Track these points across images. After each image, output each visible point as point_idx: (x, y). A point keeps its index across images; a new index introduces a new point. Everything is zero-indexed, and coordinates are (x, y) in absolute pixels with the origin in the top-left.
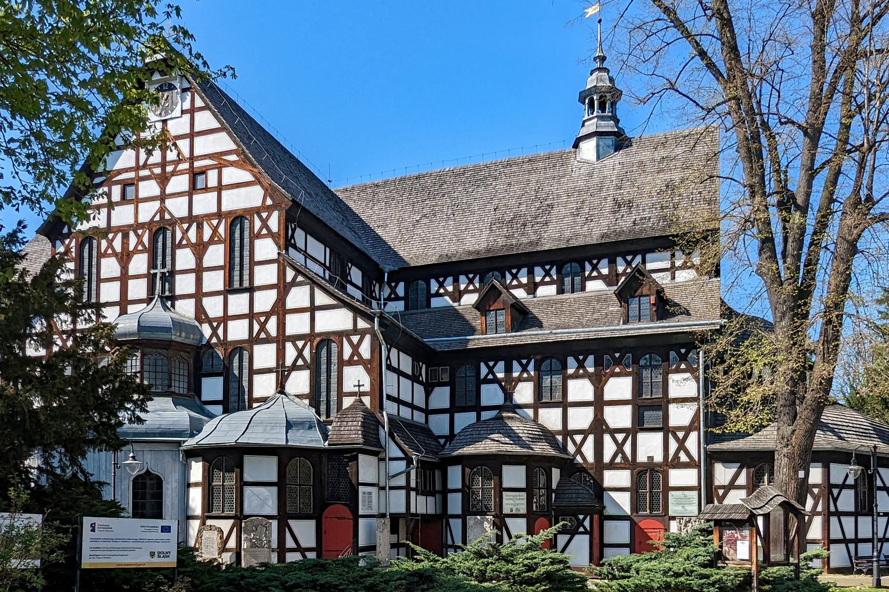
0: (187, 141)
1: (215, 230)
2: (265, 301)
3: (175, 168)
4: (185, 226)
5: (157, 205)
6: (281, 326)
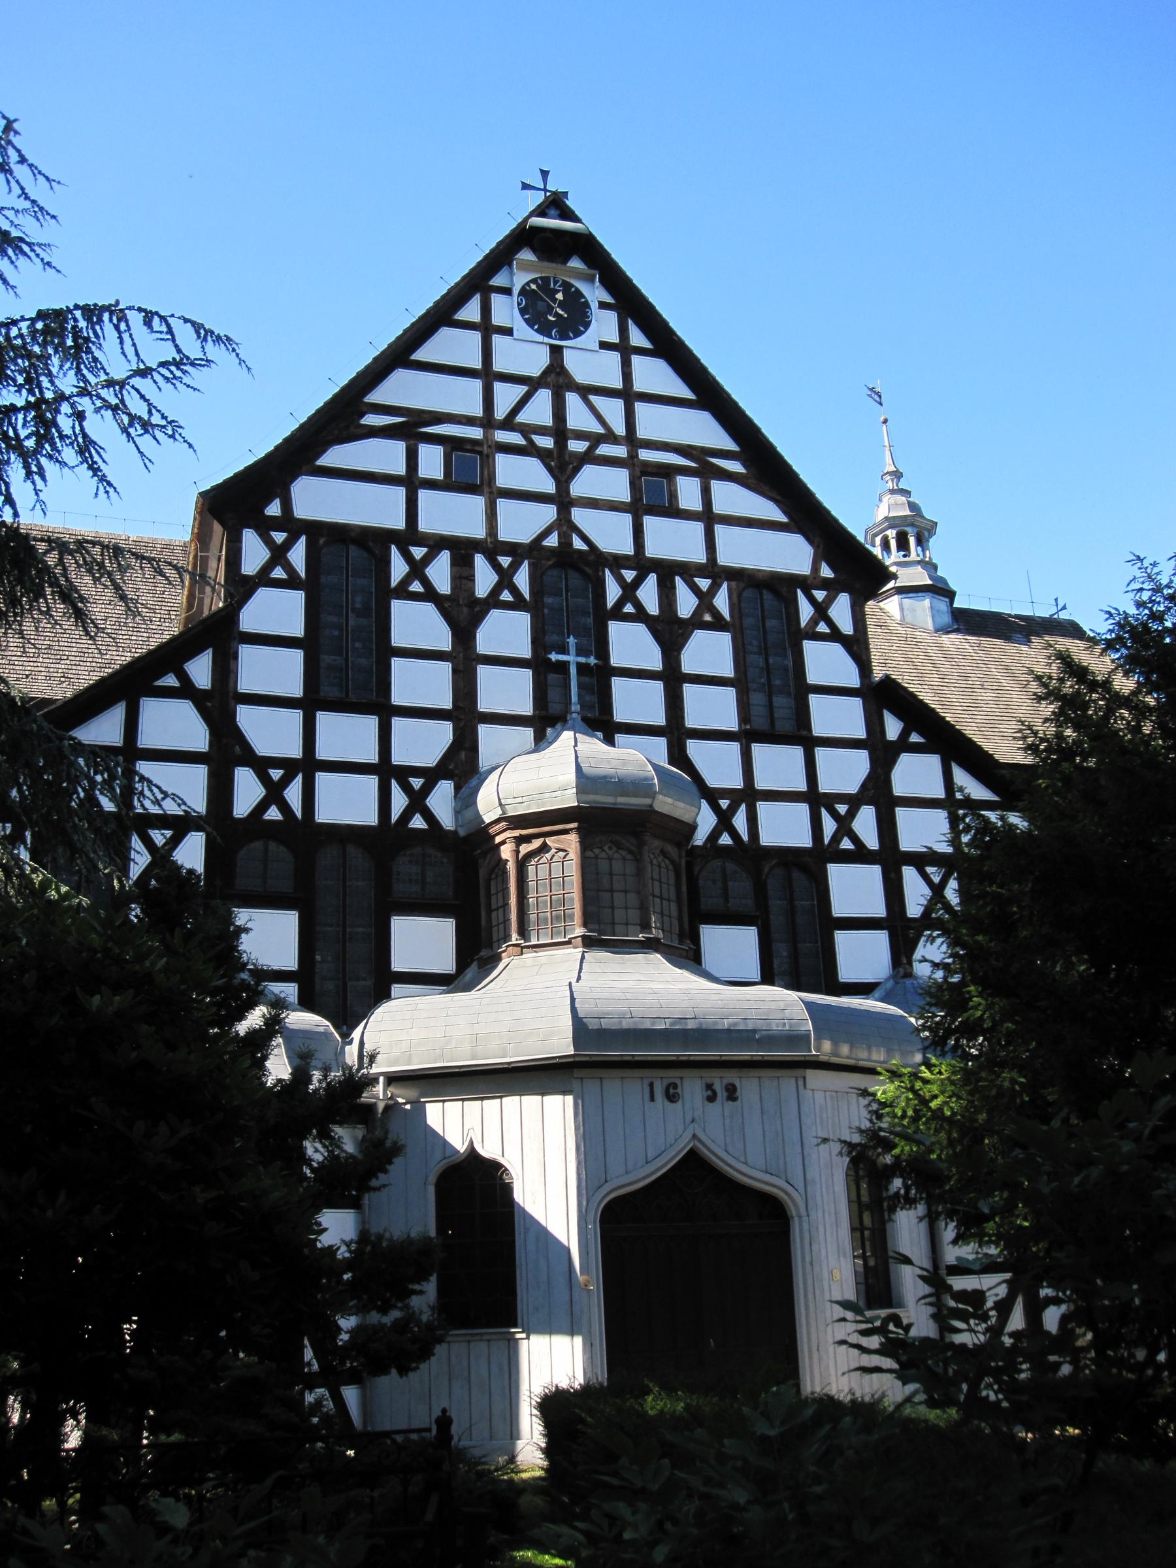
2: (844, 772)
3: (592, 449)
4: (629, 575)
5: (549, 513)
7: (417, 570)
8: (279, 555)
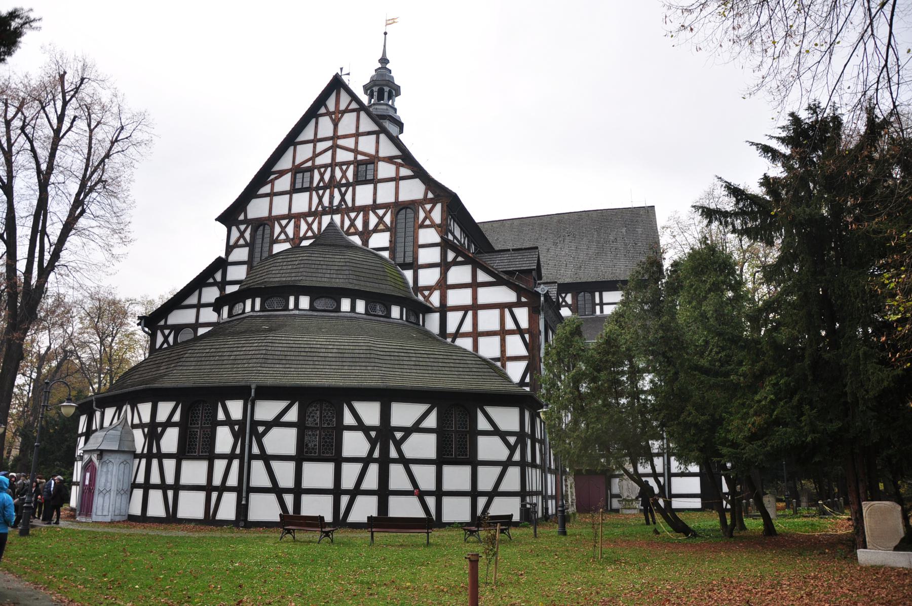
0: (352, 146)
1: (381, 219)
6: (443, 298)
7: (283, 229)
8: (242, 234)
